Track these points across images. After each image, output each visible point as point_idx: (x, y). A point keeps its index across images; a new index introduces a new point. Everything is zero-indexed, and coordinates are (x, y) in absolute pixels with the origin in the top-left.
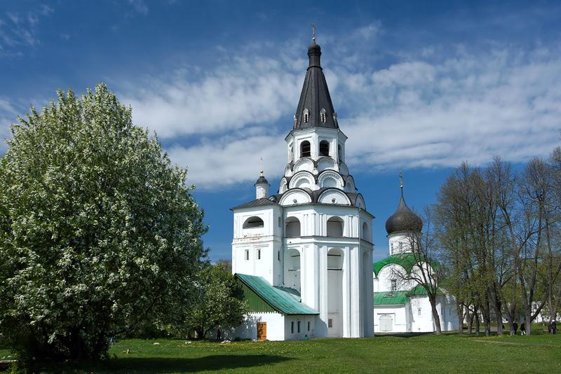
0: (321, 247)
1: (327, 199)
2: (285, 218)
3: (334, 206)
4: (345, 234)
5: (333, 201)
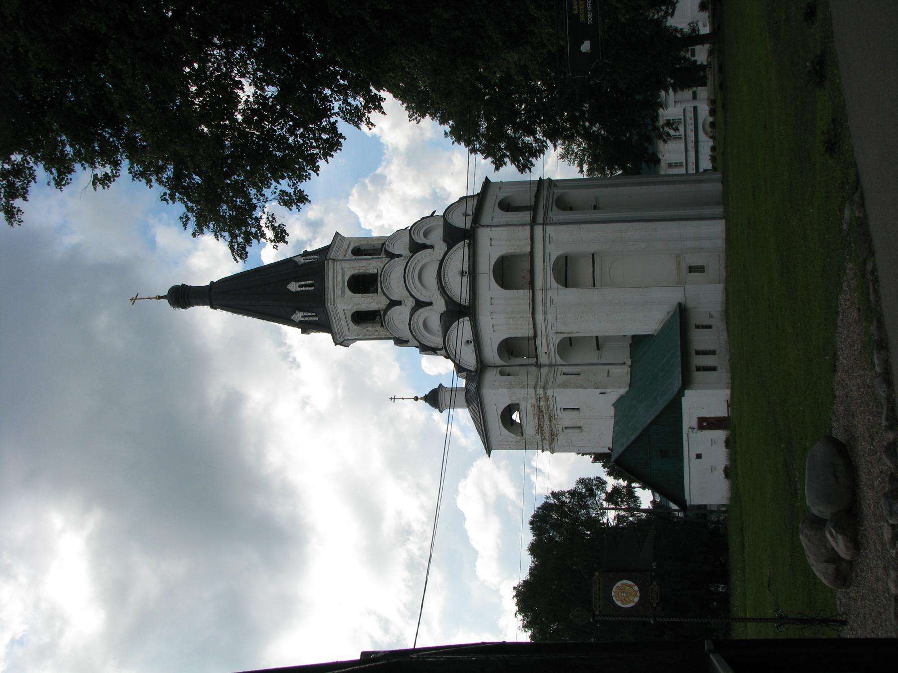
0: (552, 301)
1: (459, 288)
2: (500, 362)
3: (472, 273)
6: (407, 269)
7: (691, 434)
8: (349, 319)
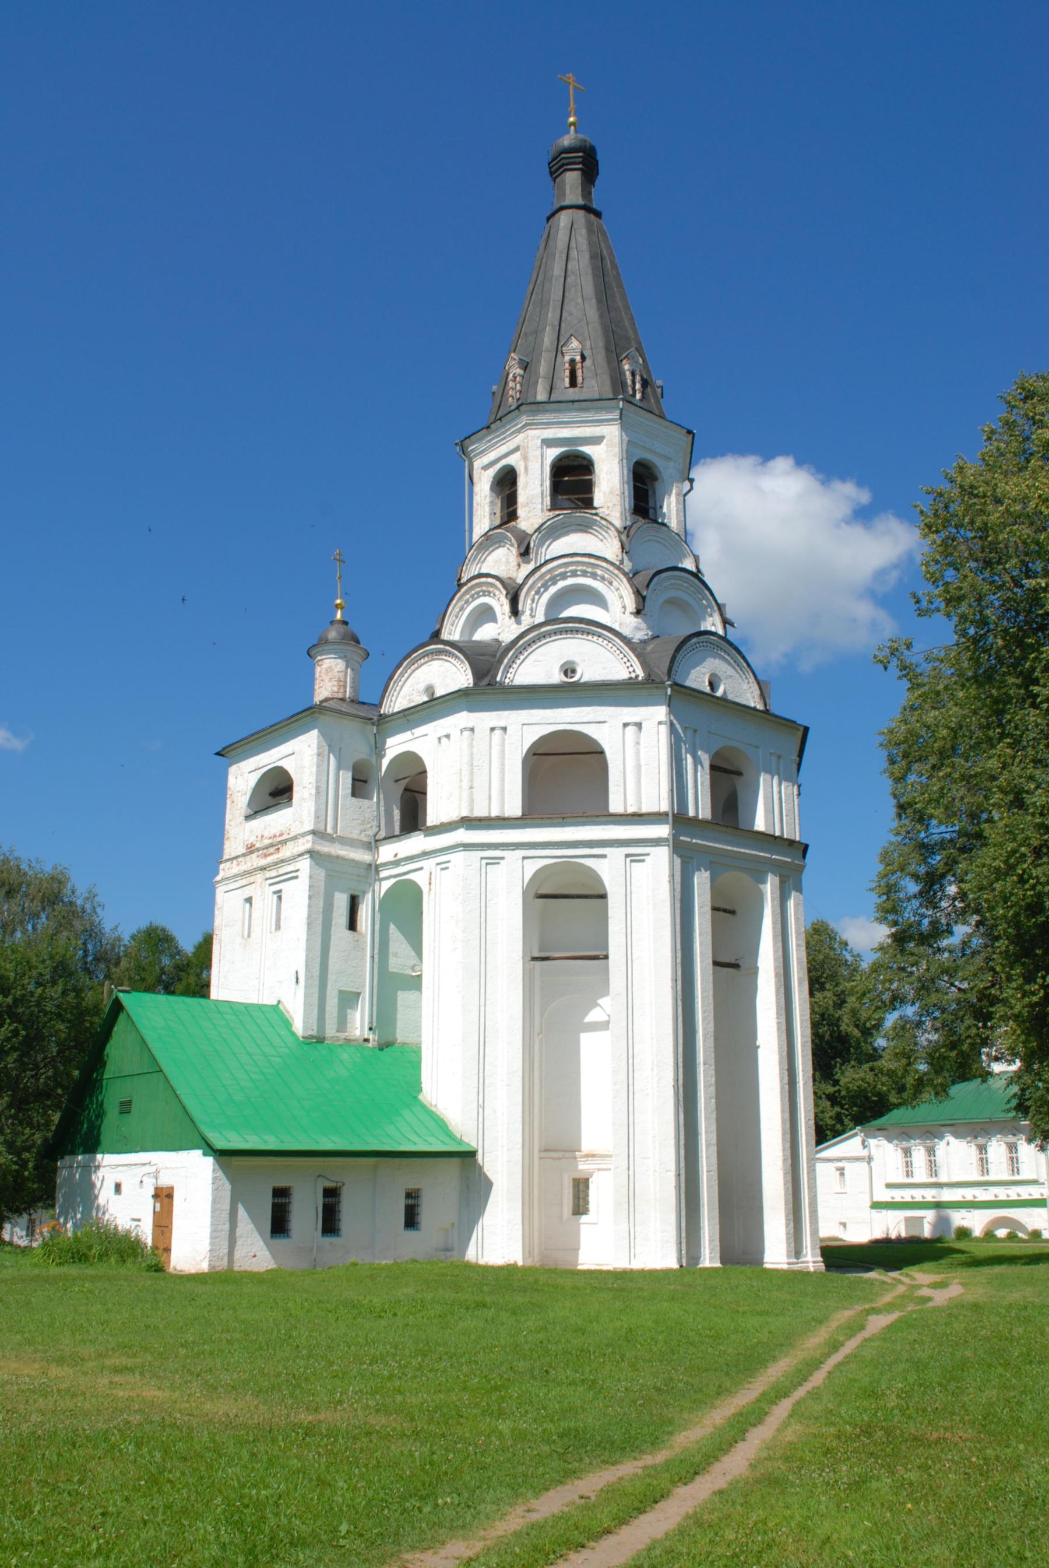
0: (496, 861)
4: (615, 805)
5: (569, 670)
6: (592, 561)
7: (147, 1169)
8: (504, 462)
